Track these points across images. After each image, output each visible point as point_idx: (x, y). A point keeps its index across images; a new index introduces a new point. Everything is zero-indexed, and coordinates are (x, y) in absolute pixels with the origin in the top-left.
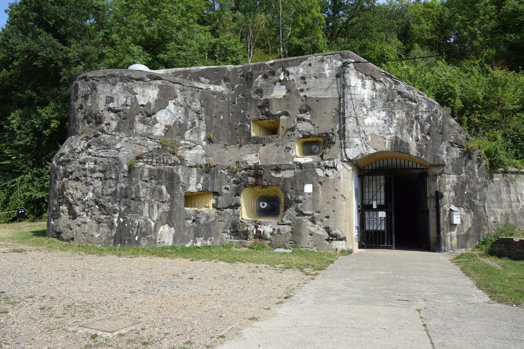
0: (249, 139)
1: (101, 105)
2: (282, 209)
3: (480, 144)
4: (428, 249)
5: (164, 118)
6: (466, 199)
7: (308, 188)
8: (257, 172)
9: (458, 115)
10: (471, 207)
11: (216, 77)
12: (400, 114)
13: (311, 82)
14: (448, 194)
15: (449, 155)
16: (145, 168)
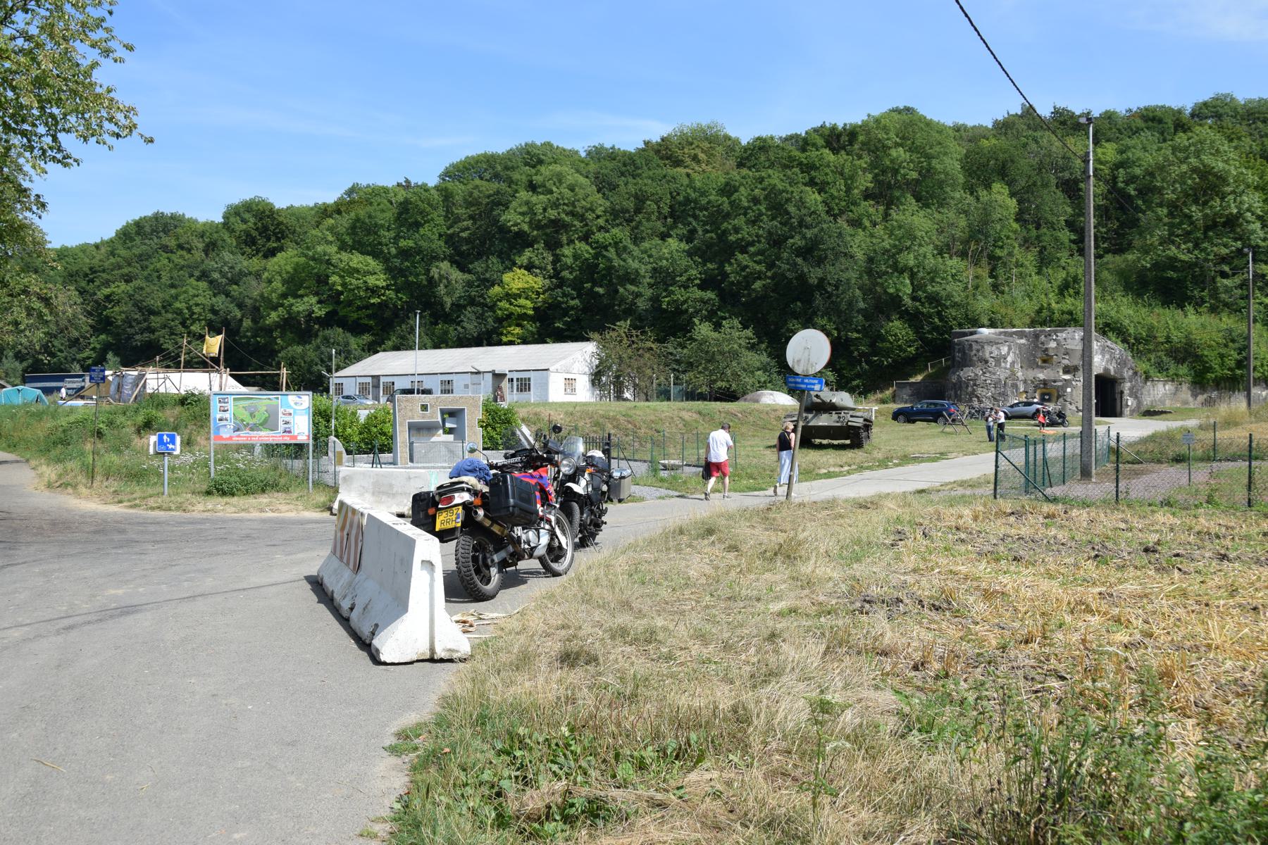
0: (1038, 366)
1: (987, 355)
2: (1054, 399)
3: (1143, 366)
4: (1115, 416)
5: (1009, 359)
6: (1134, 394)
7: (1069, 390)
8: (1045, 382)
9: (1131, 347)
10: (1136, 397)
11: (1021, 335)
12: (1107, 356)
13: (1069, 341)
14: (1126, 392)
15: (1127, 374)
16: (1010, 382)
